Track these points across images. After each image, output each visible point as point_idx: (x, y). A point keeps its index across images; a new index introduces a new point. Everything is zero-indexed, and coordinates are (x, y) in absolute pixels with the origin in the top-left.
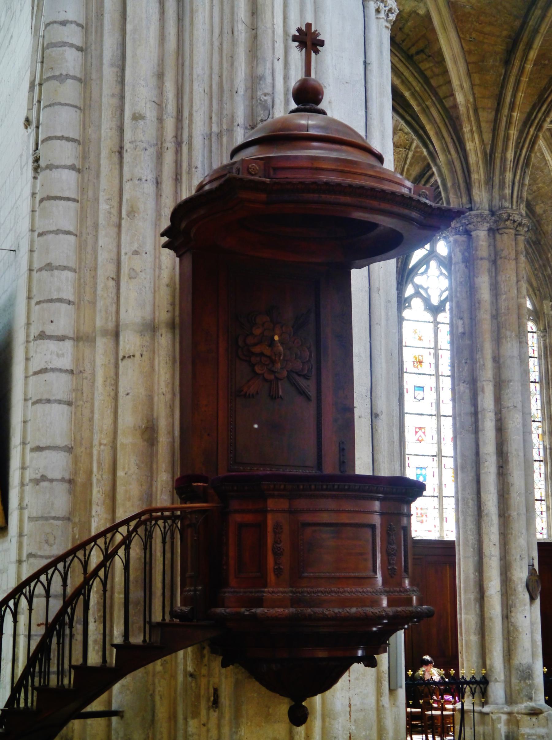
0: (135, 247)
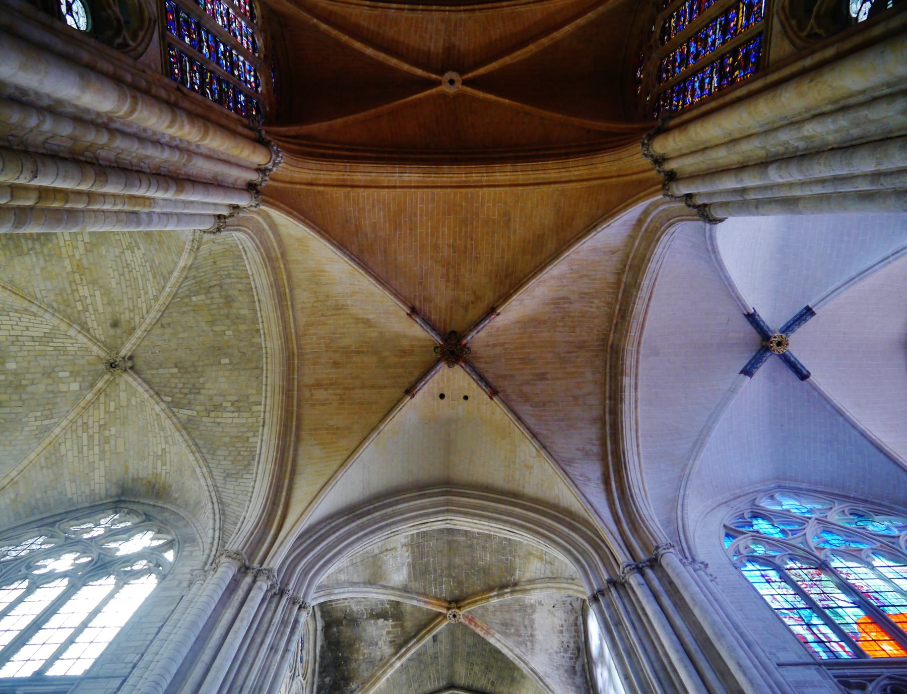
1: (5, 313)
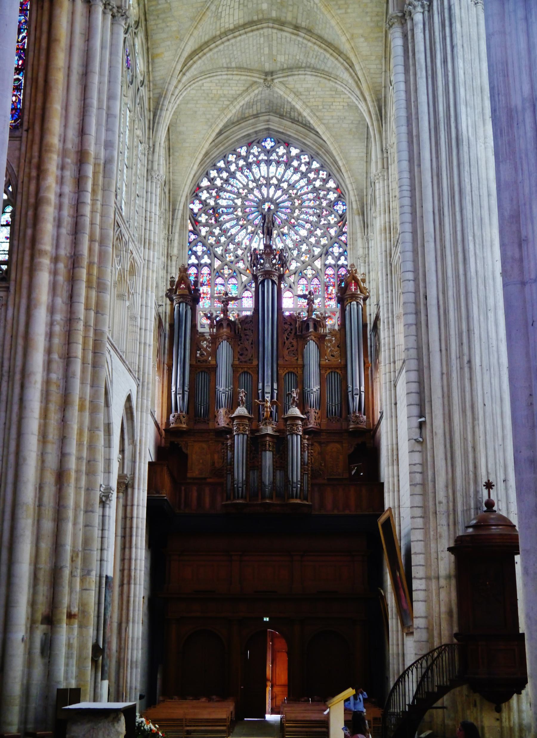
0: (442, 549)
1: (219, 14)
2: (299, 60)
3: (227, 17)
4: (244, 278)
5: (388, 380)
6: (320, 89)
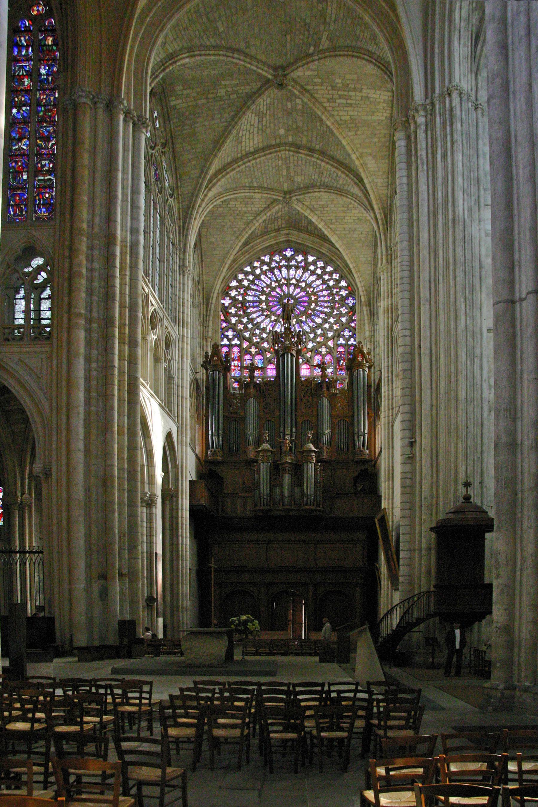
2: (314, 180)
3: (248, 140)
4: (269, 355)
5: (386, 422)
6: (333, 206)
